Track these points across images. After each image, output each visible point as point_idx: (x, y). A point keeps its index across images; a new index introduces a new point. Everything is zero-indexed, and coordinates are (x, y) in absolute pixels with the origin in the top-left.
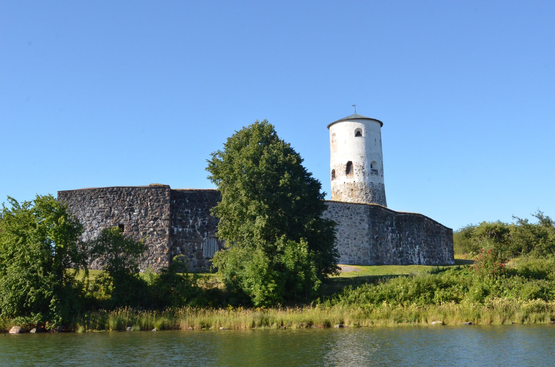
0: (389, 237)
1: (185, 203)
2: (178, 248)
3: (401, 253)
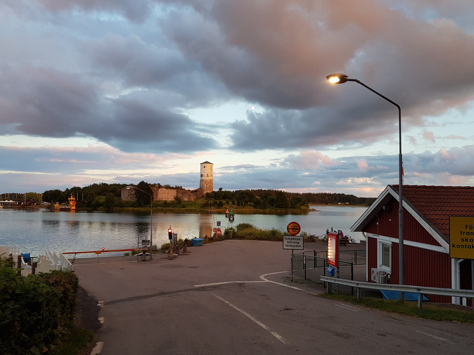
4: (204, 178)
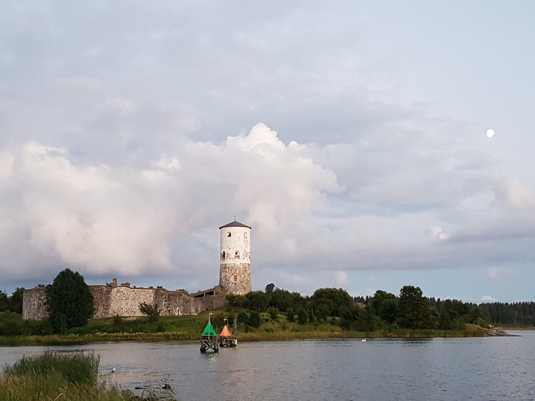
3: (169, 310)
4: (229, 262)
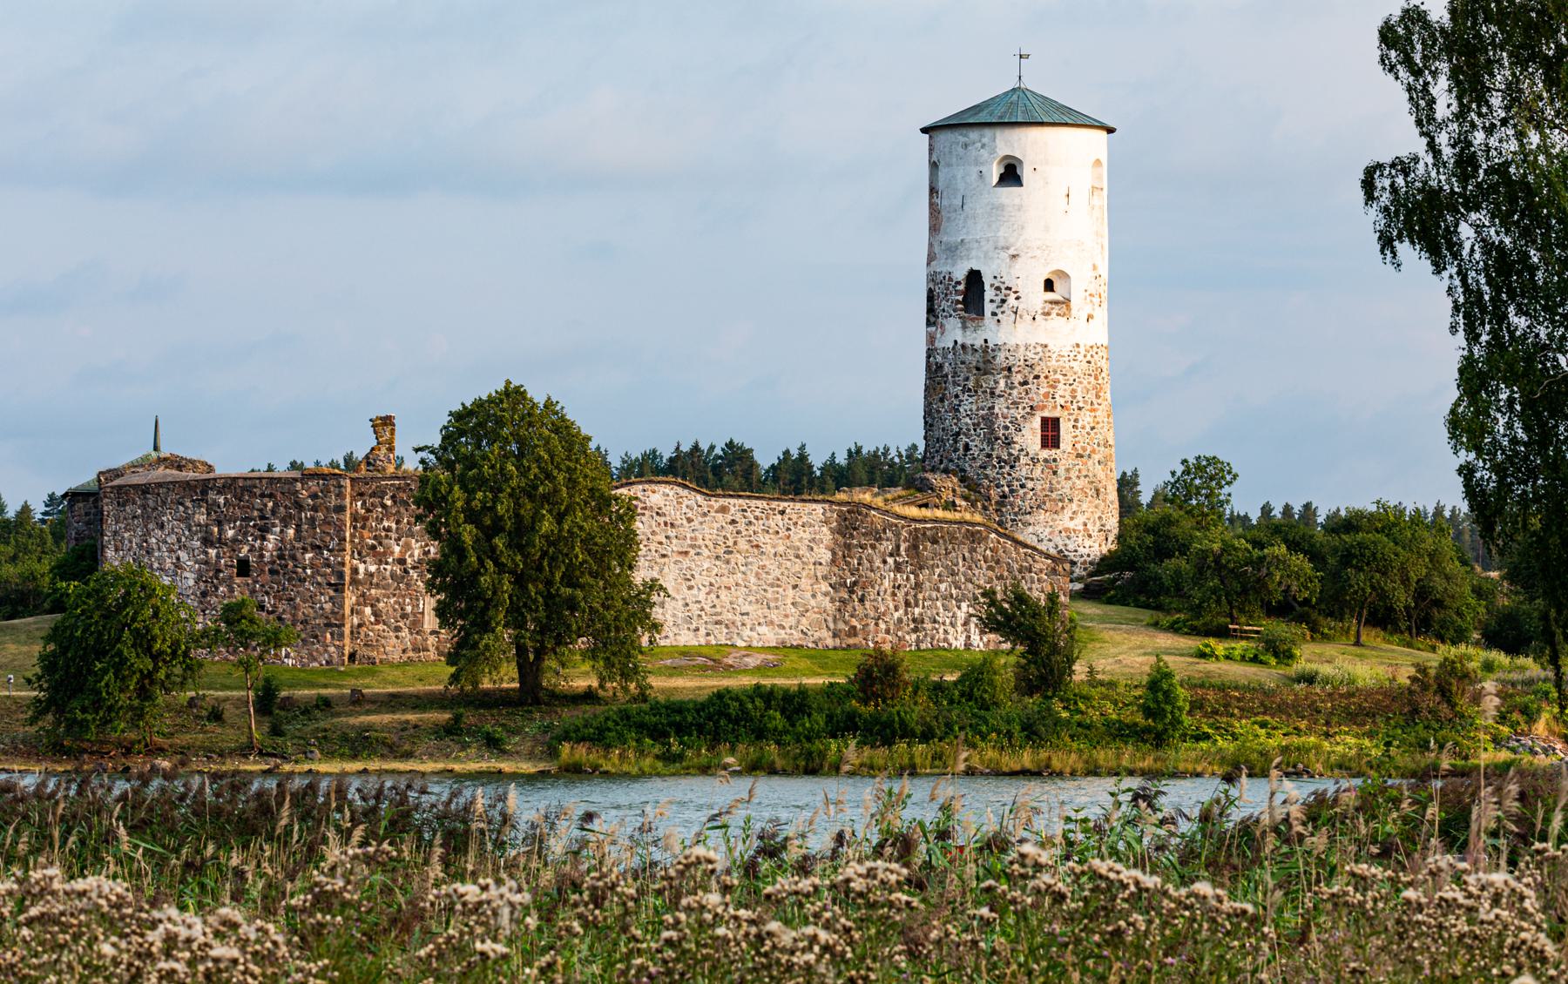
0: (886, 582)
1: (384, 506)
2: (368, 610)
